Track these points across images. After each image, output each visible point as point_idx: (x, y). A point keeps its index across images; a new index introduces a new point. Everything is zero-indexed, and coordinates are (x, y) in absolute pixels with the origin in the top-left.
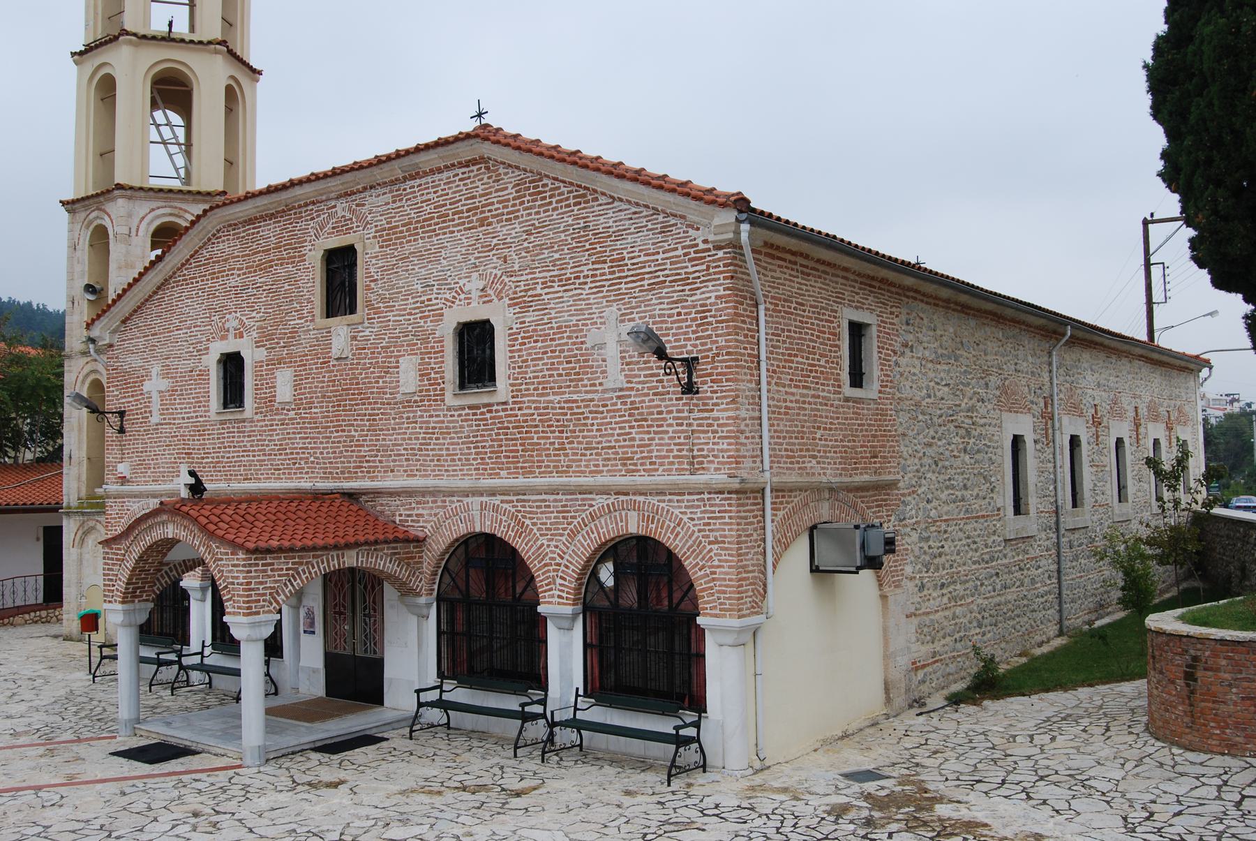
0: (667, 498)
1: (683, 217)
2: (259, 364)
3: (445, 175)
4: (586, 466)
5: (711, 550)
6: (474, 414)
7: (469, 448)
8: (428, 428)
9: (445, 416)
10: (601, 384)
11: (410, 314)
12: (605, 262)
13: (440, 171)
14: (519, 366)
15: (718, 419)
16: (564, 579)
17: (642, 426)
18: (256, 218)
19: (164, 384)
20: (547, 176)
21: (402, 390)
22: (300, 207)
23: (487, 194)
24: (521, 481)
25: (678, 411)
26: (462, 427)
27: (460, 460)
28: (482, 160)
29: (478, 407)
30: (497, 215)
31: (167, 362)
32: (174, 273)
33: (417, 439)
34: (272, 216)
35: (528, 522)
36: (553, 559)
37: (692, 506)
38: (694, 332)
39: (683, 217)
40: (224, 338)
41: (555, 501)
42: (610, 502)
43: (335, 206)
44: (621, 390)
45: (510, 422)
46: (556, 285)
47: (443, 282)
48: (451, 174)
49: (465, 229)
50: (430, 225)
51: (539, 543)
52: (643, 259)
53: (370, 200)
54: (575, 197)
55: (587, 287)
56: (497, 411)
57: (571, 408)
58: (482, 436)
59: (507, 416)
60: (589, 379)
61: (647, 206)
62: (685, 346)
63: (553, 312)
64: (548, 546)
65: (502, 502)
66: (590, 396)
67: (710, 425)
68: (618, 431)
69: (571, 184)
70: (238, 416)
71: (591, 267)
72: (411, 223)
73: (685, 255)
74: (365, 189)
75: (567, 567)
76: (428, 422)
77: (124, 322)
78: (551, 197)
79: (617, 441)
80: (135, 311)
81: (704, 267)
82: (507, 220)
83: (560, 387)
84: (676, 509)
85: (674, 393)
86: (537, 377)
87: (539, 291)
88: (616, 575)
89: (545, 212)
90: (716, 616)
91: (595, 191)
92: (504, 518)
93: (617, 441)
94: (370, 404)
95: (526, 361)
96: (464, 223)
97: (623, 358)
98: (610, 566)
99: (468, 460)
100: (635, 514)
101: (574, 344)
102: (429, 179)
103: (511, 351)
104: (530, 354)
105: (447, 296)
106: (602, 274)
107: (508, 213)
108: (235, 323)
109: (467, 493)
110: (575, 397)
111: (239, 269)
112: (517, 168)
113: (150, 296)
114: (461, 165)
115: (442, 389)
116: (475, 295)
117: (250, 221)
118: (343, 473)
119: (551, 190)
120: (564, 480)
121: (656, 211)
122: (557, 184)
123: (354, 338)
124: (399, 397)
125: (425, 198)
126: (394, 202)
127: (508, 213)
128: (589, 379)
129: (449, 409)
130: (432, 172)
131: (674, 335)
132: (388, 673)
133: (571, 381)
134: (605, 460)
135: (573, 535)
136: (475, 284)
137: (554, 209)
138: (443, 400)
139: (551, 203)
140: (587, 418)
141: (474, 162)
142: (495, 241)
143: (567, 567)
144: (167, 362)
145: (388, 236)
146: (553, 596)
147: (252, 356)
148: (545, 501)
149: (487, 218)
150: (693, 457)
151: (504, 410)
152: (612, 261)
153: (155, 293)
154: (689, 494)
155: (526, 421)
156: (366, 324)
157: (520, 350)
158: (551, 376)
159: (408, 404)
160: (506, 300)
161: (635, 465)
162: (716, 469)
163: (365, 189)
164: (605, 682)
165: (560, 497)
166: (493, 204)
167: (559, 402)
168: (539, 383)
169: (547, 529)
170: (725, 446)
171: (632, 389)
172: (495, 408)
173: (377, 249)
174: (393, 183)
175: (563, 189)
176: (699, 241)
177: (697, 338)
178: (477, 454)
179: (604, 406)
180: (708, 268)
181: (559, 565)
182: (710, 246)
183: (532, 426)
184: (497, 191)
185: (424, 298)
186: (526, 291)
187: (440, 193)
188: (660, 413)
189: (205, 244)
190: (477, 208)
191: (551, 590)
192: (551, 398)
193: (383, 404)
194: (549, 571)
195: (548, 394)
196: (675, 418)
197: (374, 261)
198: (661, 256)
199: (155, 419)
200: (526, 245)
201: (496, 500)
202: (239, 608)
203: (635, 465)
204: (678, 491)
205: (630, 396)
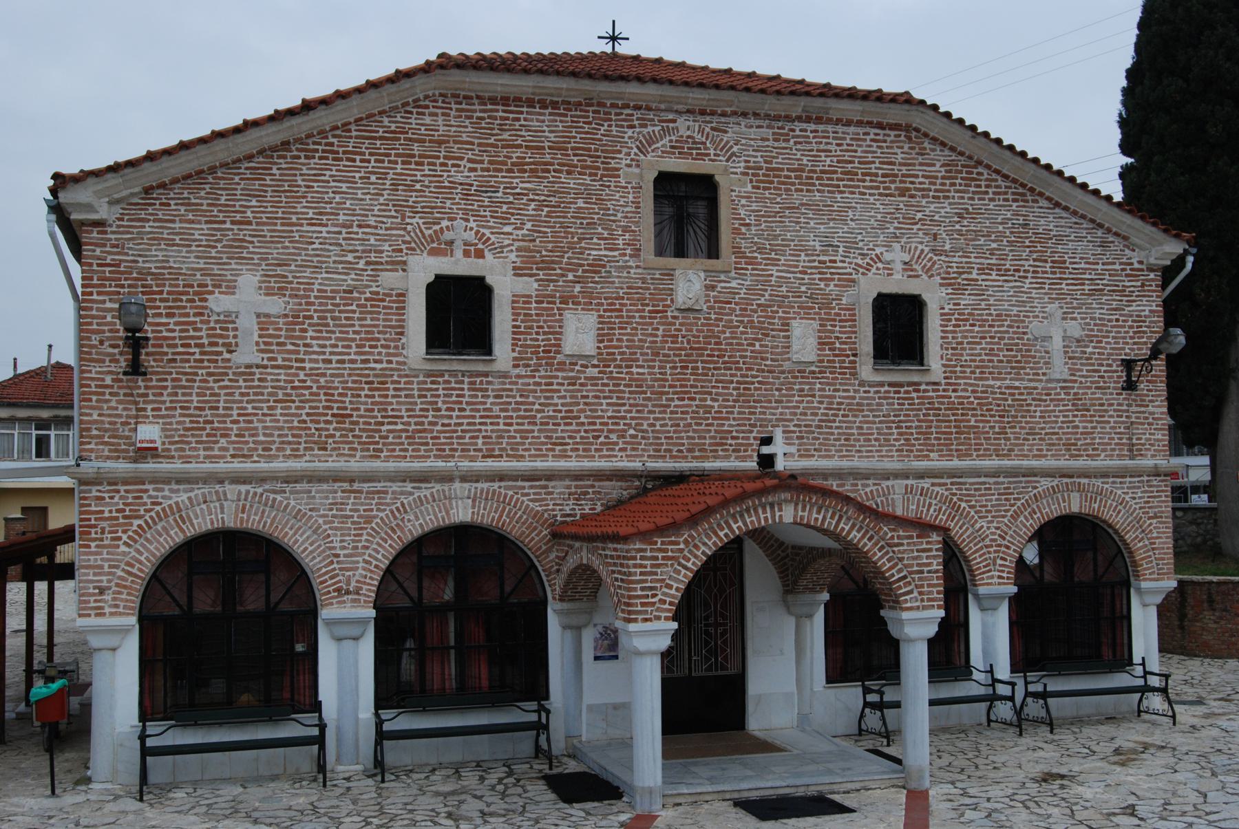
0: (1111, 480)
1: (1125, 238)
2: (520, 302)
3: (852, 129)
4: (1030, 450)
5: (1150, 524)
6: (896, 392)
7: (891, 428)
8: (832, 403)
9: (855, 391)
10: (1044, 374)
11: (805, 273)
12: (1046, 261)
13: (849, 123)
14: (953, 348)
15: (1153, 413)
16: (1005, 560)
17: (1085, 416)
18: (518, 99)
19: (275, 305)
20: (988, 167)
21: (795, 358)
22: (613, 106)
23: (910, 165)
24: (956, 463)
25: (1119, 405)
26: (878, 404)
27: (876, 440)
28: (908, 128)
29: (901, 385)
30: (923, 190)
31: (279, 271)
32: (308, 136)
33: (816, 414)
34: (555, 105)
35: (963, 505)
36: (995, 540)
37: (1134, 487)
38: (1131, 338)
39: (1125, 238)
40: (434, 252)
41: (995, 483)
42: (1054, 484)
43: (674, 121)
44: (1065, 381)
45: (943, 403)
46: (994, 273)
47: (851, 246)
48: (861, 130)
49: (880, 194)
50: (832, 179)
51: (978, 526)
52: (1083, 266)
53: (736, 128)
54: (1013, 194)
55: (1027, 281)
56: (925, 391)
57: (1013, 394)
58: (905, 415)
59: (938, 397)
60: (1031, 368)
61: (1092, 221)
62: (1124, 349)
63: (992, 299)
64: (988, 528)
65: (933, 485)
66: (1032, 384)
67: (1147, 418)
68: (1061, 419)
69: (1015, 181)
70: (481, 368)
71: (1031, 262)
72: (803, 171)
73: (1123, 270)
74: (734, 113)
75: (1008, 547)
76: (835, 397)
77: (148, 190)
78: (987, 186)
79: (1061, 428)
80: (189, 176)
81: (1139, 284)
82: (934, 197)
83: (1000, 373)
84: (1121, 489)
85: (1115, 388)
86: (974, 361)
87: (974, 276)
88: (1041, 555)
89: (980, 199)
90: (1157, 580)
91: (1041, 194)
92: (934, 502)
93: (1061, 428)
94: (741, 369)
95: (962, 343)
96: (878, 188)
97: (1066, 352)
98: (1035, 544)
99: (889, 440)
100: (1077, 495)
101: (1014, 333)
102: (830, 128)
103: (943, 331)
104: (966, 337)
105: (860, 262)
106: (1046, 272)
107: (936, 191)
108: (470, 236)
109: (897, 475)
110: (1017, 384)
111: (470, 161)
112: (952, 149)
113: (239, 160)
114: (880, 126)
115: (855, 362)
116: (899, 266)
117: (505, 101)
118: (689, 450)
119: (987, 180)
120: (1006, 463)
121: (1101, 226)
122: (994, 176)
123: (713, 288)
124: (787, 365)
125: (822, 147)
126: (775, 140)
127: (936, 191)
128: (1031, 368)
129: (862, 384)
130: (838, 121)
131: (1114, 338)
132: (755, 686)
133: (1012, 368)
134: (1050, 445)
135: (1015, 516)
136: (897, 256)
137: (990, 200)
138: (854, 374)
139: (987, 193)
140: (1030, 405)
141: (893, 127)
142: (919, 215)
143: (1008, 547)
144: (279, 271)
145: (766, 177)
146: (992, 577)
147: (506, 286)
148: (985, 483)
149: (909, 189)
150: (1133, 445)
151: (934, 391)
152: (1052, 262)
153: (250, 157)
154: (1131, 476)
155: (962, 403)
156: (733, 274)
157: (955, 332)
158: (990, 361)
159: (801, 371)
160: (938, 279)
161: (1079, 450)
162: (1153, 456)
163: (734, 113)
164: (1026, 656)
165: (1001, 479)
166: (917, 176)
167: (1000, 388)
168: (977, 367)
169: (987, 511)
170: (1160, 437)
171: (1075, 381)
172: (923, 387)
173: (749, 188)
174: (777, 118)
175: (1000, 183)
176: (1134, 261)
177: (1135, 343)
178: (899, 434)
179: (1047, 394)
180: (1143, 285)
181: (1000, 546)
182: (1144, 267)
183: (969, 409)
184: (921, 164)
185: (827, 258)
186: (961, 273)
187: (845, 147)
188: (1102, 405)
189: (392, 109)
190: (896, 176)
191: (990, 571)
192: (991, 383)
193: (763, 371)
194: (989, 553)
195: (987, 379)
196: (1115, 410)
197: (743, 201)
198: (1100, 267)
199: (247, 354)
200: (957, 227)
201: (926, 483)
202: (929, 600)
203: (1079, 450)
204: (1121, 473)
205: (1073, 388)
